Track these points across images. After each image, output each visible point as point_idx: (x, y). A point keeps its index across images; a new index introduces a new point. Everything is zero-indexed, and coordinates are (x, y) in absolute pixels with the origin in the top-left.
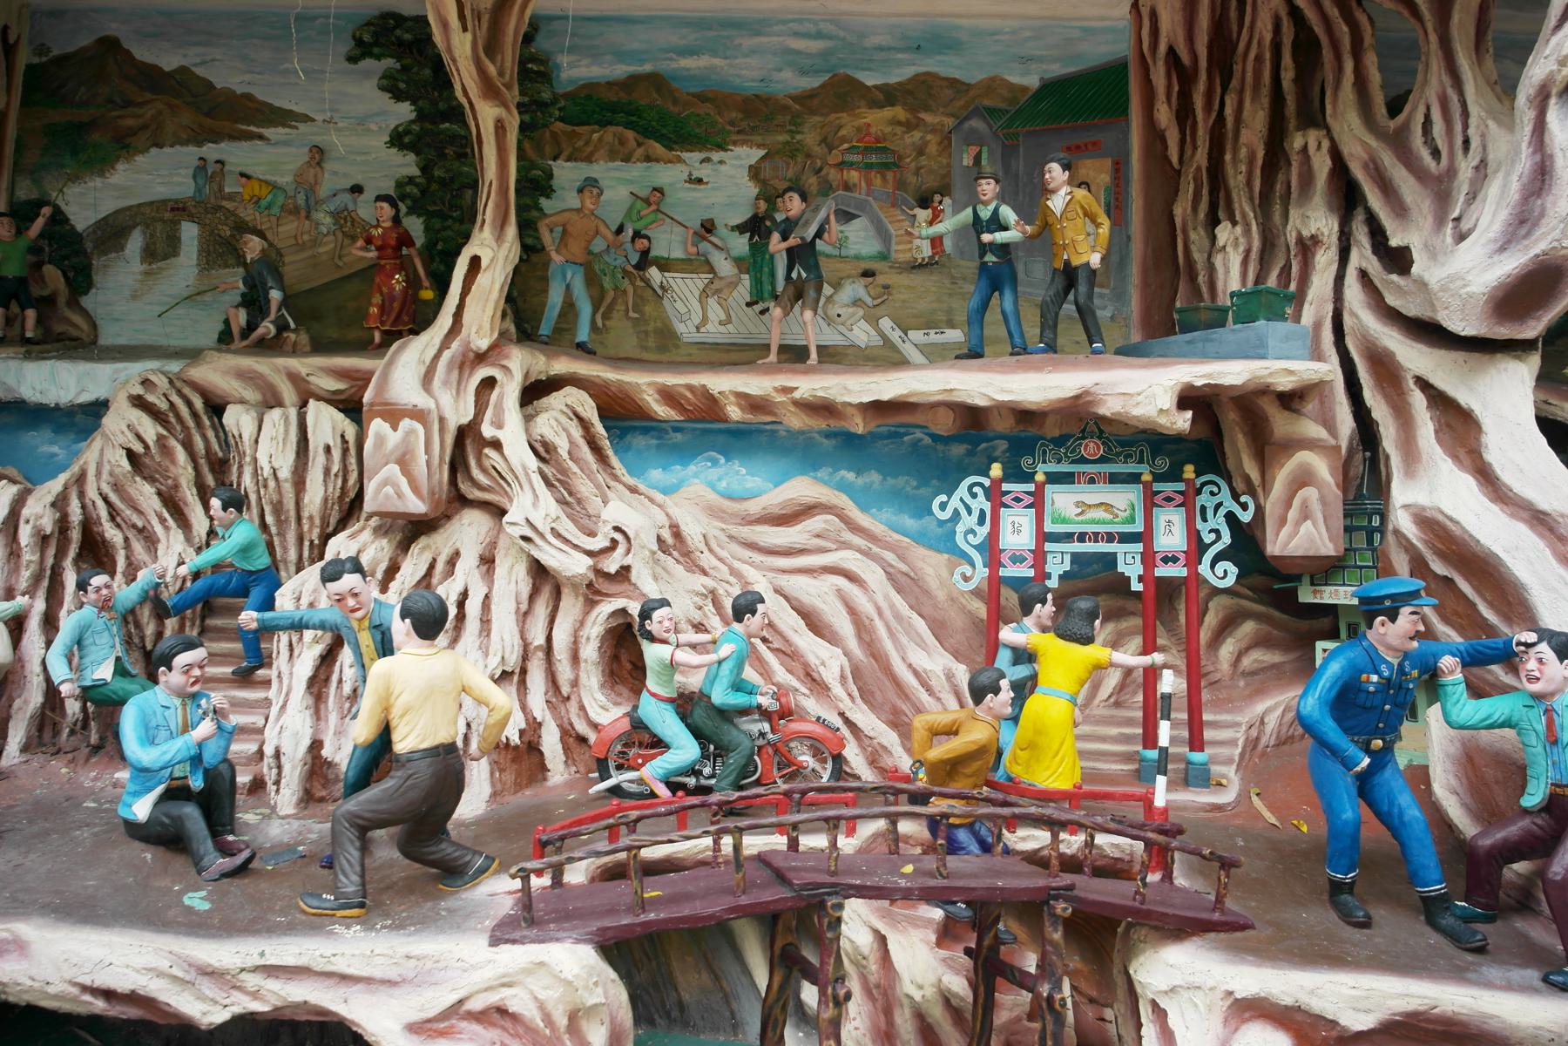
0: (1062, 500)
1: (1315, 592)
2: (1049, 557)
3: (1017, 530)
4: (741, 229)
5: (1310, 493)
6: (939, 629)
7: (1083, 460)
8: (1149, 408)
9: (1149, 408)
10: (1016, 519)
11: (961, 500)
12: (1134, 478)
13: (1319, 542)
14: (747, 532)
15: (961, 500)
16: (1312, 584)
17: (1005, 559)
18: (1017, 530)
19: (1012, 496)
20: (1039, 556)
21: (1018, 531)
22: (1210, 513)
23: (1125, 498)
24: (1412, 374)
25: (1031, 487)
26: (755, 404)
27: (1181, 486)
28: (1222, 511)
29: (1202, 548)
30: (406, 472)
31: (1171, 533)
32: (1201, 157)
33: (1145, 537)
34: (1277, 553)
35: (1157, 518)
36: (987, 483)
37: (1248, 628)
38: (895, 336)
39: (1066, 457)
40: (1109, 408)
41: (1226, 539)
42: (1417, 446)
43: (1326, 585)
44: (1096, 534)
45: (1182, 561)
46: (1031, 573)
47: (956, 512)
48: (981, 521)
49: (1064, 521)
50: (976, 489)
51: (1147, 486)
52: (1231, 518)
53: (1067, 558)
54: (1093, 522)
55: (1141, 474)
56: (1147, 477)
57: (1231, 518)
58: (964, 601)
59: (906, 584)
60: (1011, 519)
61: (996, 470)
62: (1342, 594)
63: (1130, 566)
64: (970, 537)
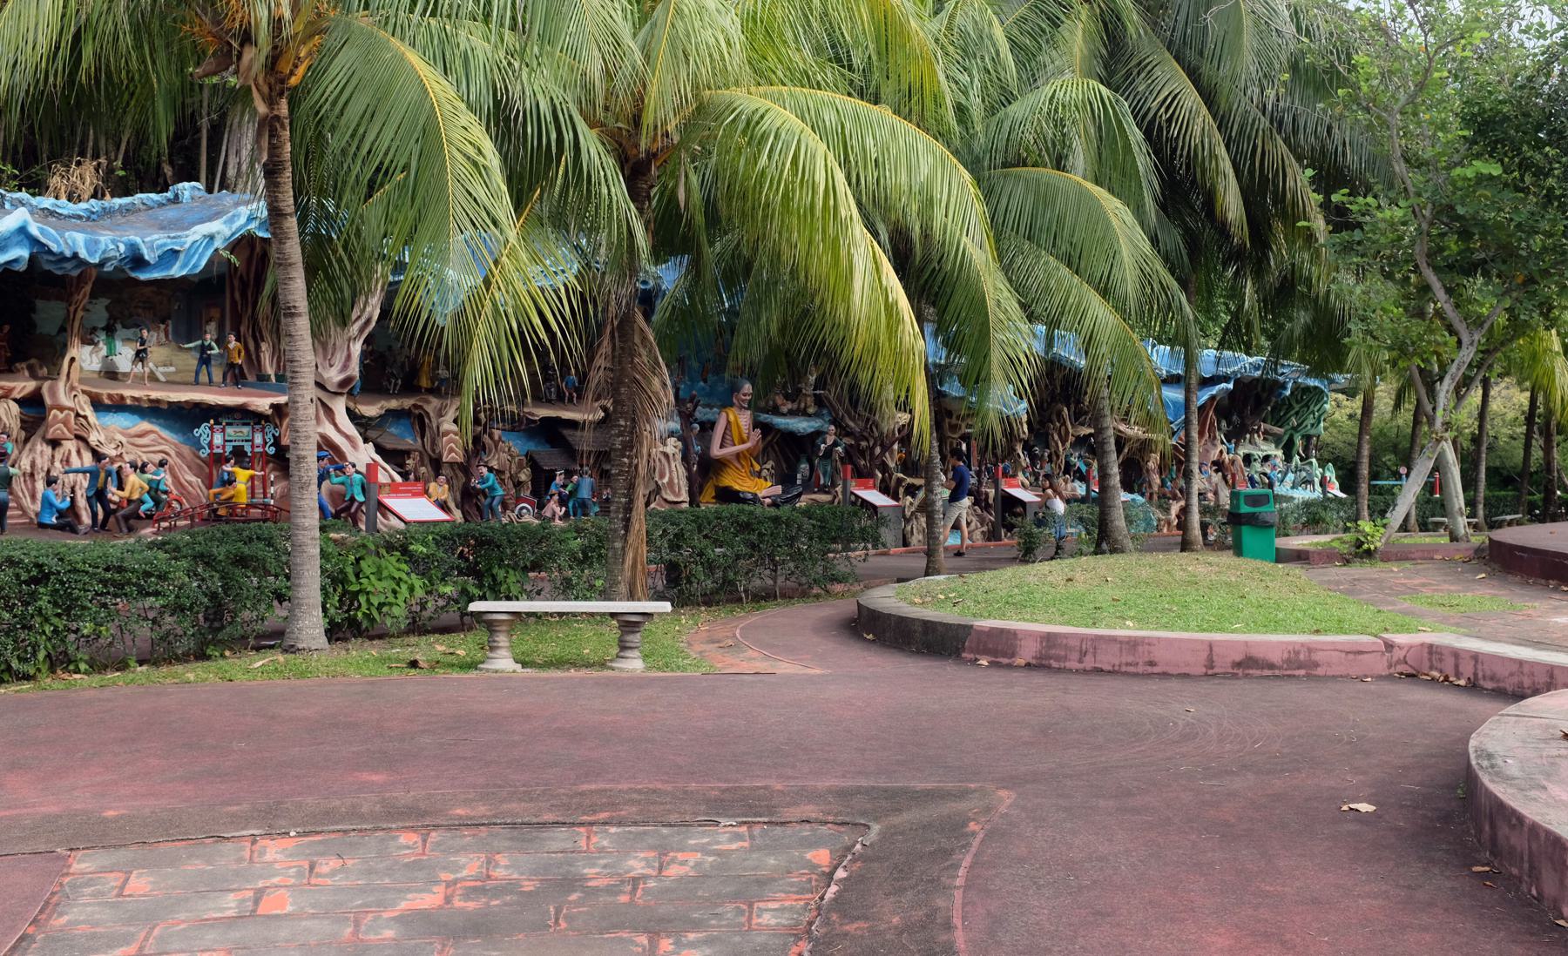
0: (230, 430)
4: (103, 329)
6: (189, 467)
12: (248, 424)
14: (132, 440)
20: (224, 447)
21: (218, 439)
23: (246, 430)
26: (134, 398)
30: (65, 425)
31: (258, 440)
32: (250, 311)
33: (252, 441)
37: (271, 465)
38: (154, 369)
40: (252, 408)
59: (179, 454)
61: (212, 421)
63: (248, 449)
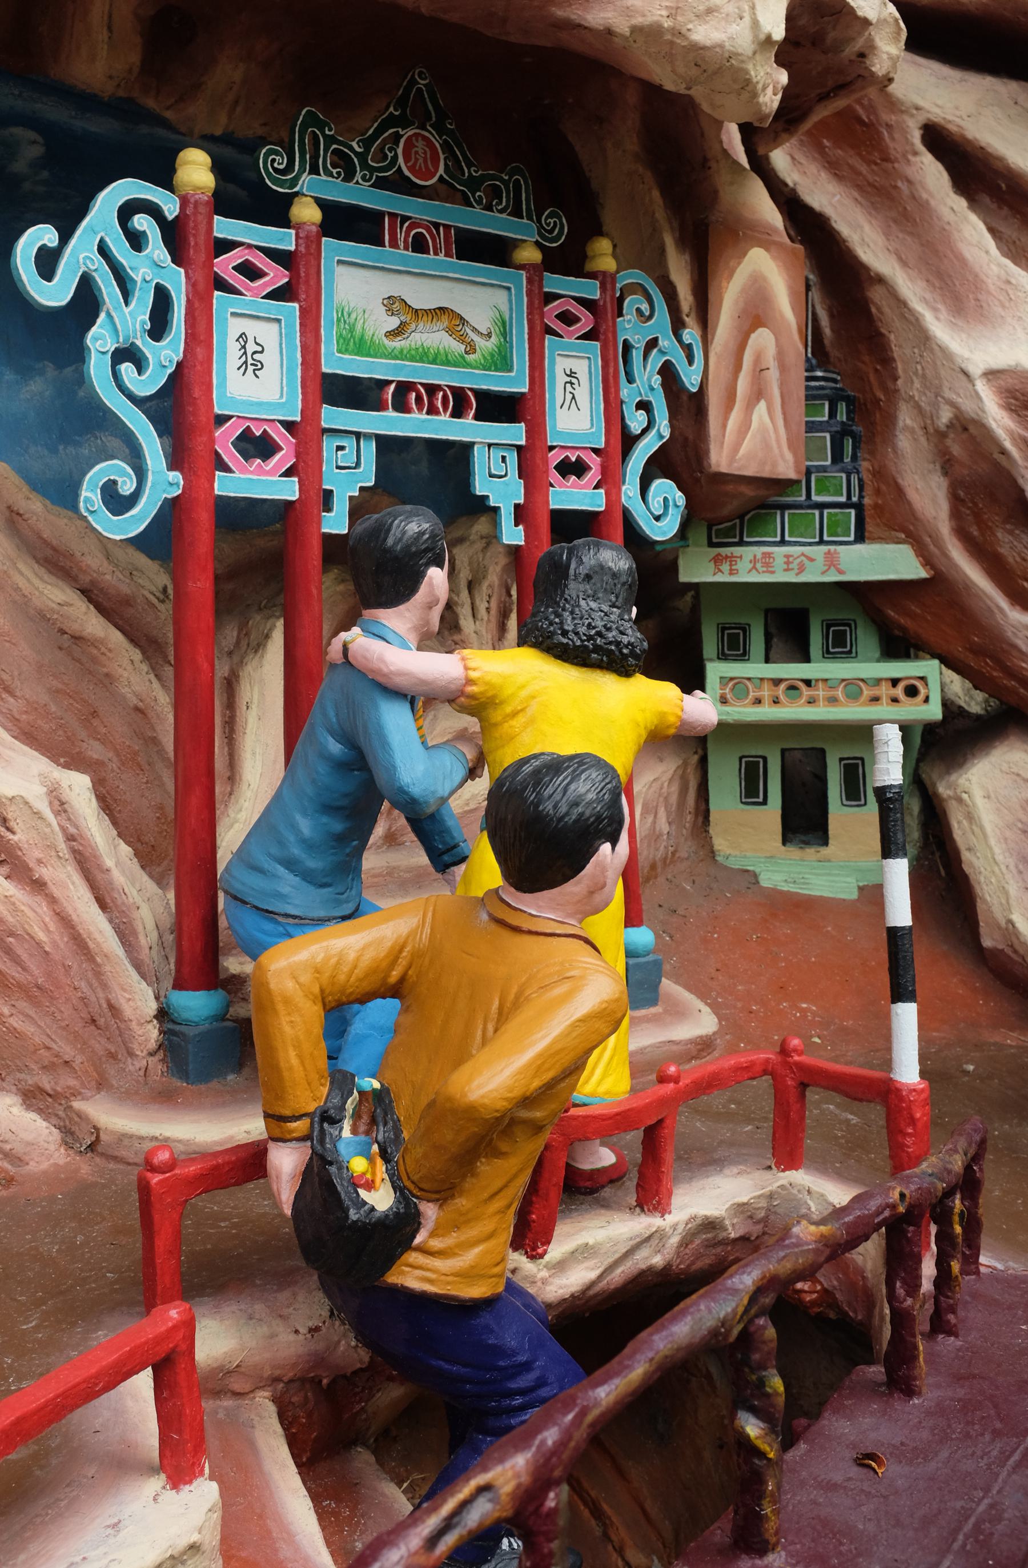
1: (717, 560)
2: (329, 444)
3: (252, 364)
5: (763, 339)
7: (400, 185)
8: (734, 29)
9: (734, 29)
10: (254, 329)
11: (103, 250)
13: (776, 451)
15: (103, 250)
16: (711, 544)
17: (224, 441)
18: (252, 364)
19: (236, 257)
22: (637, 356)
24: (921, 118)
25: (285, 240)
27: (591, 290)
28: (656, 361)
29: (629, 441)
34: (724, 469)
35: (553, 363)
36: (171, 208)
39: (364, 165)
41: (663, 426)
42: (963, 262)
43: (741, 543)
44: (432, 389)
45: (593, 475)
46: (289, 490)
47: (86, 286)
48: (158, 328)
49: (362, 347)
50: (142, 222)
51: (535, 273)
52: (668, 372)
53: (369, 450)
54: (423, 356)
55: (515, 244)
56: (530, 254)
57: (668, 372)
58: (22, 583)
60: (236, 327)
62: (779, 562)
64: (127, 369)
